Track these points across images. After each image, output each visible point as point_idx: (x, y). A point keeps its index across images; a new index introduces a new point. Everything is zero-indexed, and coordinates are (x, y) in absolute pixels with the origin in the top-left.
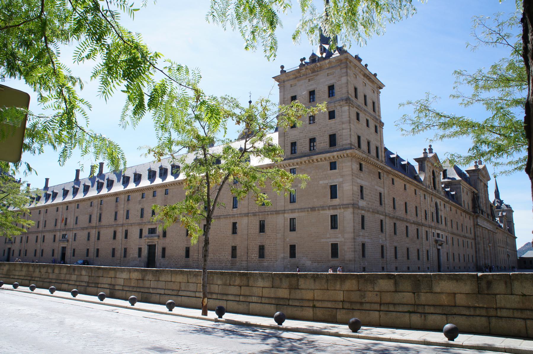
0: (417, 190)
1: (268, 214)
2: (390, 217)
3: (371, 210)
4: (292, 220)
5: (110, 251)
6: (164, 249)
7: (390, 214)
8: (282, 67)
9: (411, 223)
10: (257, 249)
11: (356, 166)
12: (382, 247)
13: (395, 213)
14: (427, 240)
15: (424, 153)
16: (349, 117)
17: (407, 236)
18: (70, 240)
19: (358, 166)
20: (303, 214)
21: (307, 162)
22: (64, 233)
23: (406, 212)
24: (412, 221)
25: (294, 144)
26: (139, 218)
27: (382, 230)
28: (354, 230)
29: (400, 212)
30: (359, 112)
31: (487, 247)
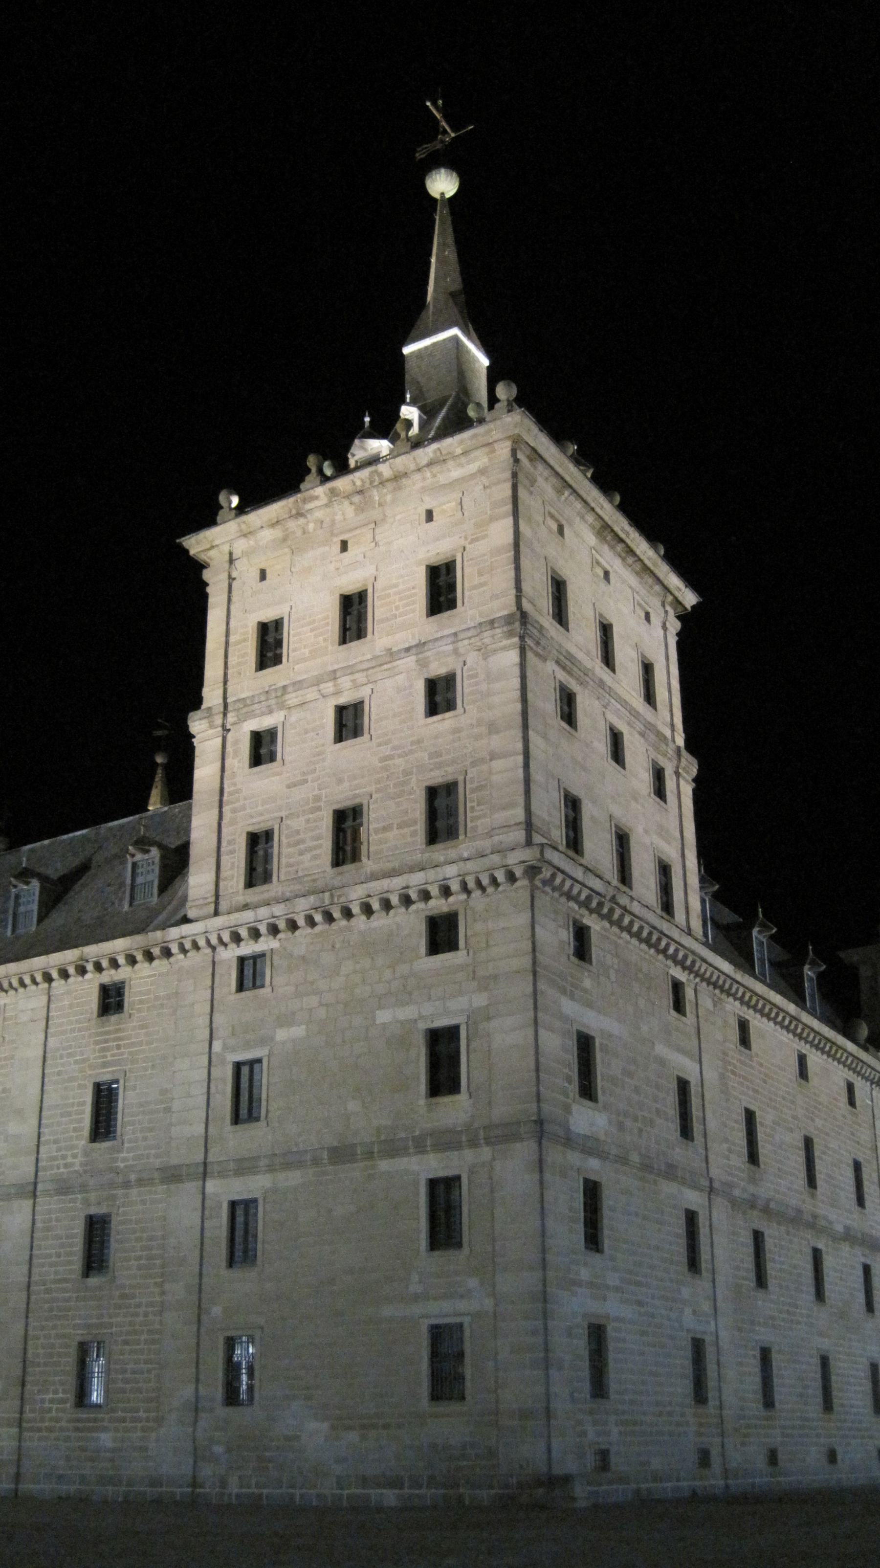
0: (860, 1085)
1: (127, 1185)
2: (734, 1203)
3: (635, 1158)
4: (242, 1213)
7: (731, 1185)
9: (836, 1238)
11: (556, 937)
12: (698, 1347)
13: (753, 1180)
17: (820, 1294)
19: (566, 936)
20: (293, 1178)
21: (318, 918)
23: (812, 1181)
27: (693, 1264)
29: (781, 1177)
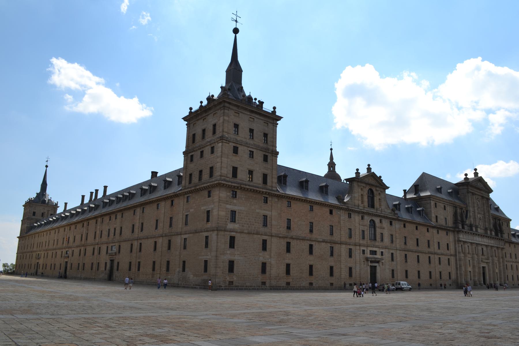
5: (90, 266)
6: (118, 263)
8: (191, 109)
9: (319, 242)
10: (165, 264)
14: (350, 256)
15: (356, 173)
16: (222, 152)
18: (70, 256)
20: (191, 235)
22: (67, 250)
24: (321, 240)
25: (191, 175)
26: (107, 238)
28: (217, 249)
30: (238, 146)
31: (479, 263)
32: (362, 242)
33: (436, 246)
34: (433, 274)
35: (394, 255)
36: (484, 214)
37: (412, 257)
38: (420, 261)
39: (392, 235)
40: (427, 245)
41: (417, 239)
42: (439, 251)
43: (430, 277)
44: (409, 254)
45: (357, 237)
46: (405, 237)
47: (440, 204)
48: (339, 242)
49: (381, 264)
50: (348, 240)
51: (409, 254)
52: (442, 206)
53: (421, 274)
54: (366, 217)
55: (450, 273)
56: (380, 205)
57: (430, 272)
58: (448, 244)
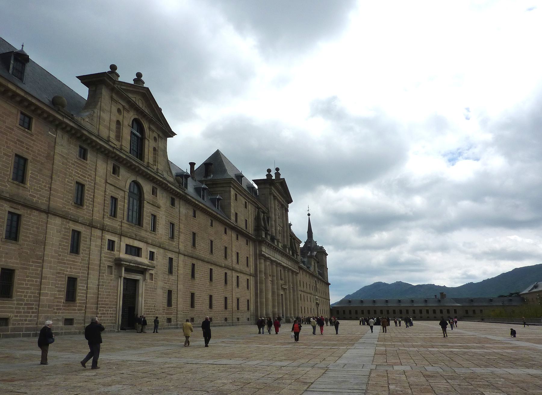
32: (108, 222)
33: (235, 257)
34: (229, 301)
35: (175, 264)
36: (283, 226)
37: (202, 270)
38: (213, 278)
39: (172, 225)
40: (224, 255)
41: (212, 242)
42: (237, 267)
43: (226, 308)
44: (199, 265)
45: (96, 207)
46: (194, 234)
47: (242, 198)
48: (44, 207)
49: (148, 276)
50: (72, 210)
51: (199, 265)
52: (244, 201)
53: (214, 302)
54: (123, 171)
55: (248, 300)
56: (155, 161)
57: (226, 298)
58: (247, 257)
